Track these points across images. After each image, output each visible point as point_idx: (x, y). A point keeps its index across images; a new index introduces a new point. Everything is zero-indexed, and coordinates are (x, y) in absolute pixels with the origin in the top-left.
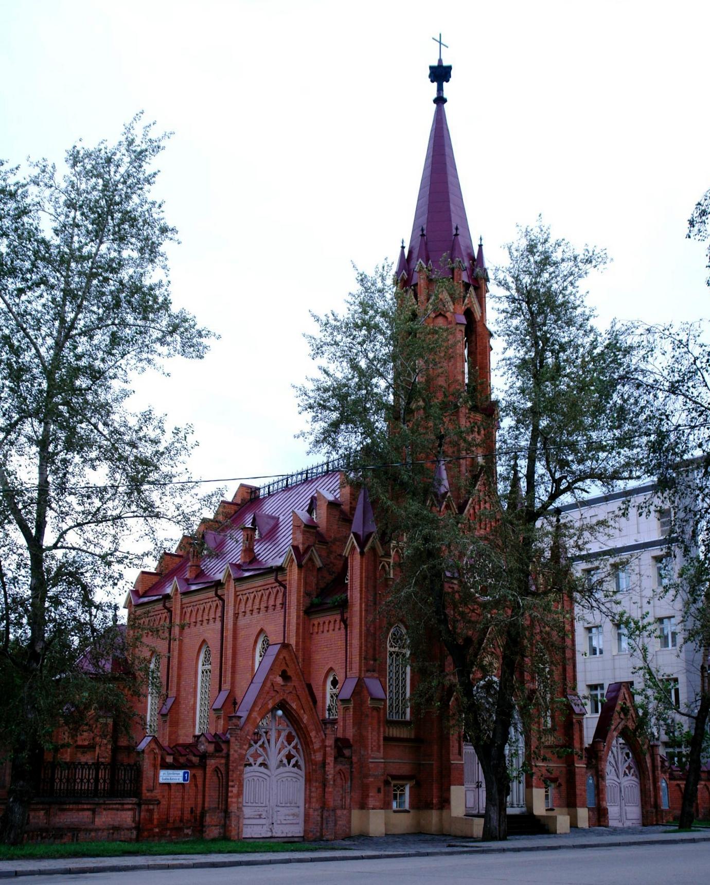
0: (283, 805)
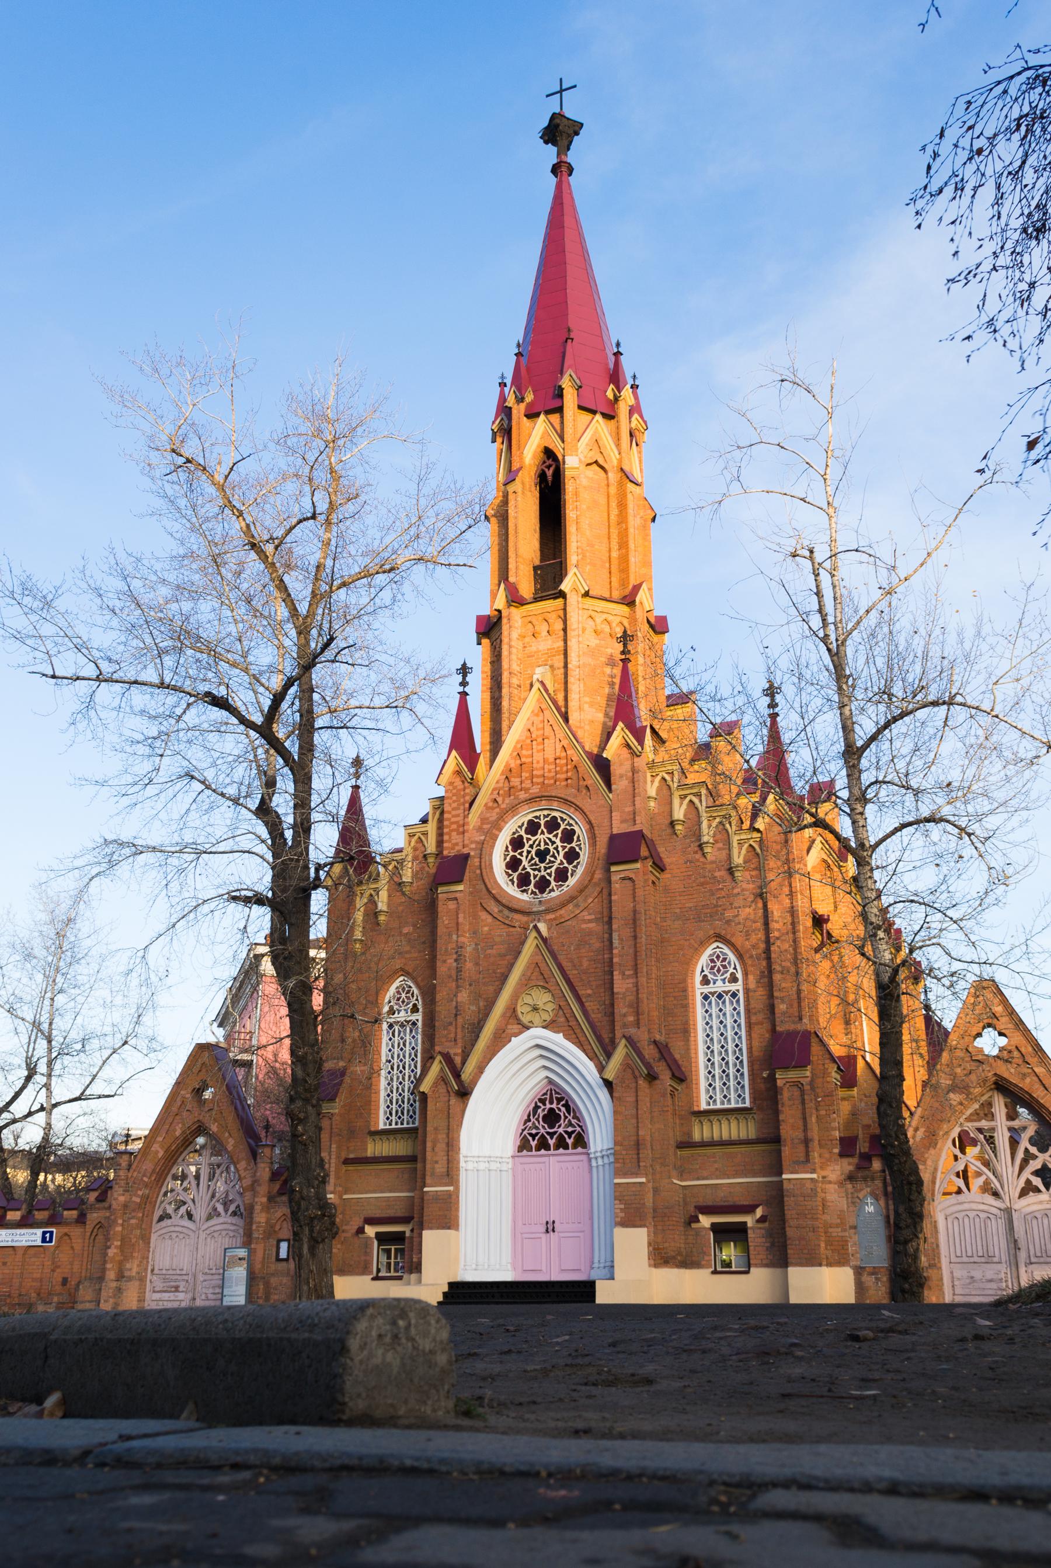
0: (214, 1271)
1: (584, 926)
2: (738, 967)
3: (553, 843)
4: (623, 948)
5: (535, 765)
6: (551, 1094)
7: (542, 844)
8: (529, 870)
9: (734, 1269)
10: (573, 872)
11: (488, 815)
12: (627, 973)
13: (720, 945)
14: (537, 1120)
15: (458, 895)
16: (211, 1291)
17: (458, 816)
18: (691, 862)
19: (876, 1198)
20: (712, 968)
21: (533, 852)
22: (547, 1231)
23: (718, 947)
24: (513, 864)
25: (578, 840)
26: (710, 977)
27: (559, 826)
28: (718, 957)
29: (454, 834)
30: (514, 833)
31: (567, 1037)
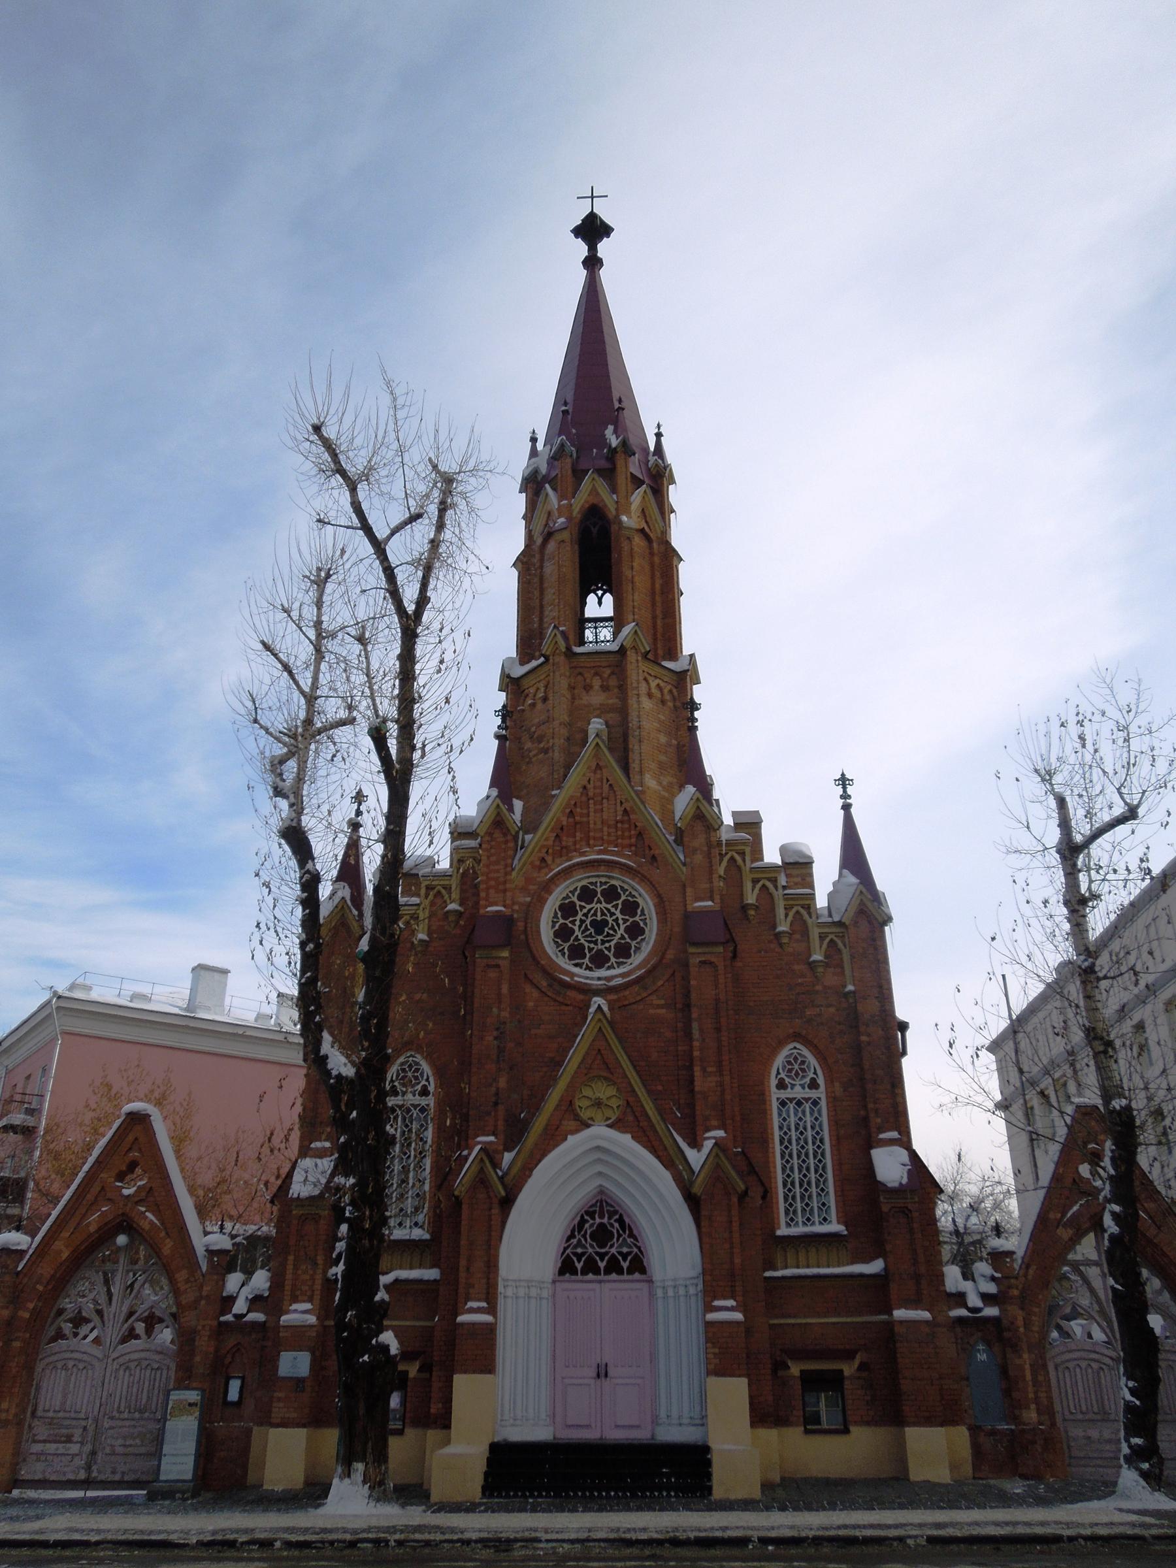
0: (126, 1415)
1: (652, 1011)
2: (819, 1071)
3: (612, 914)
4: (704, 1040)
5: (592, 826)
6: (601, 1207)
7: (599, 914)
8: (582, 941)
9: (825, 1426)
10: (638, 949)
11: (535, 875)
12: (709, 1069)
13: (798, 1046)
14: (584, 1236)
15: (500, 962)
16: (120, 1442)
17: (498, 871)
18: (766, 952)
19: (989, 1344)
20: (790, 1071)
21: (588, 922)
22: (598, 1376)
23: (795, 1048)
24: (563, 934)
25: (643, 913)
26: (787, 1080)
27: (619, 897)
28: (796, 1059)
29: (492, 891)
30: (564, 899)
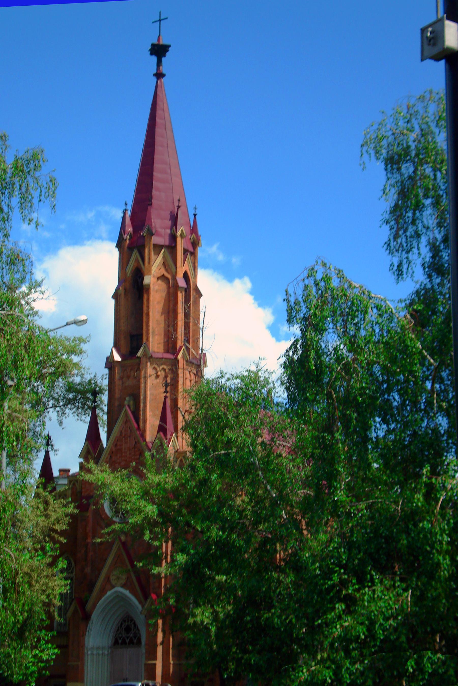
31: (130, 592)
